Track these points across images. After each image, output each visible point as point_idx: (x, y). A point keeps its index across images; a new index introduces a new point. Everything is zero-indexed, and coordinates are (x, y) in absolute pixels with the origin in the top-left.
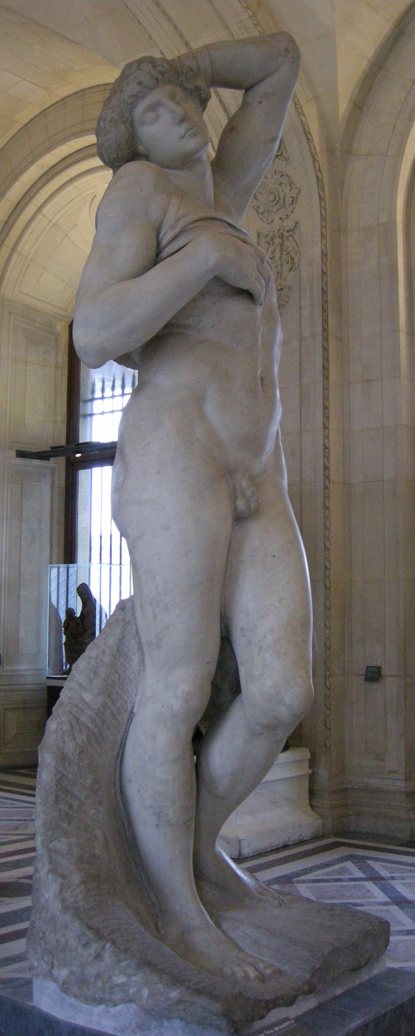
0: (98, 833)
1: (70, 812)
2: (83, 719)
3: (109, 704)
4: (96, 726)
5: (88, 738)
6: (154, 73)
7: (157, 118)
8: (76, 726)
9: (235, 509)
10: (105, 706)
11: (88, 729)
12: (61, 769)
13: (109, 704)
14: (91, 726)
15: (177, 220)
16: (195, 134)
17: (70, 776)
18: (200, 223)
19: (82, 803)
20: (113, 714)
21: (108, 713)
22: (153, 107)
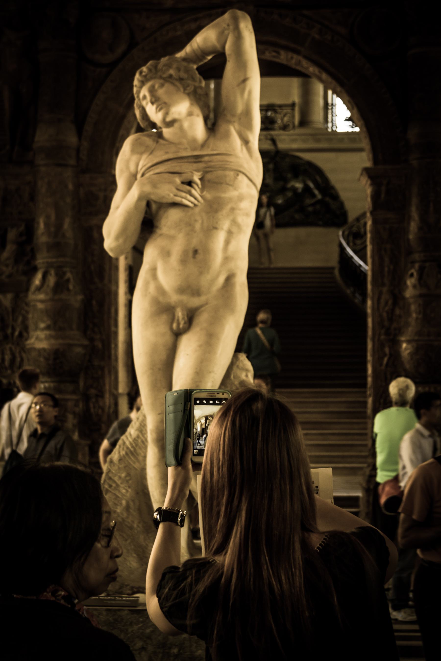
0: (124, 502)
1: (109, 489)
2: (127, 443)
3: (141, 436)
4: (133, 447)
5: (127, 453)
6: (140, 78)
7: (147, 104)
8: (122, 446)
9: (171, 328)
10: (138, 437)
11: (128, 448)
12: (109, 467)
13: (141, 436)
14: (130, 447)
15: (141, 169)
16: (160, 109)
17: (114, 472)
18: (153, 168)
19: (118, 485)
20: (143, 442)
21: (140, 441)
22: (145, 97)
